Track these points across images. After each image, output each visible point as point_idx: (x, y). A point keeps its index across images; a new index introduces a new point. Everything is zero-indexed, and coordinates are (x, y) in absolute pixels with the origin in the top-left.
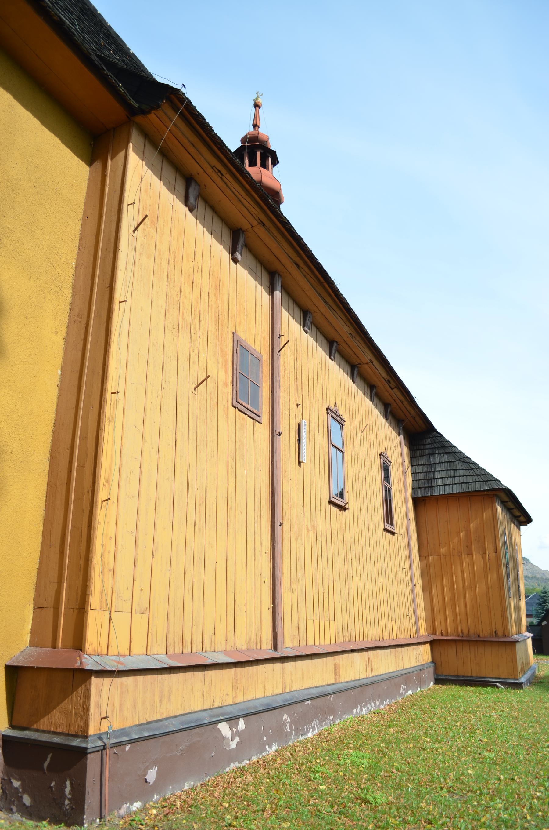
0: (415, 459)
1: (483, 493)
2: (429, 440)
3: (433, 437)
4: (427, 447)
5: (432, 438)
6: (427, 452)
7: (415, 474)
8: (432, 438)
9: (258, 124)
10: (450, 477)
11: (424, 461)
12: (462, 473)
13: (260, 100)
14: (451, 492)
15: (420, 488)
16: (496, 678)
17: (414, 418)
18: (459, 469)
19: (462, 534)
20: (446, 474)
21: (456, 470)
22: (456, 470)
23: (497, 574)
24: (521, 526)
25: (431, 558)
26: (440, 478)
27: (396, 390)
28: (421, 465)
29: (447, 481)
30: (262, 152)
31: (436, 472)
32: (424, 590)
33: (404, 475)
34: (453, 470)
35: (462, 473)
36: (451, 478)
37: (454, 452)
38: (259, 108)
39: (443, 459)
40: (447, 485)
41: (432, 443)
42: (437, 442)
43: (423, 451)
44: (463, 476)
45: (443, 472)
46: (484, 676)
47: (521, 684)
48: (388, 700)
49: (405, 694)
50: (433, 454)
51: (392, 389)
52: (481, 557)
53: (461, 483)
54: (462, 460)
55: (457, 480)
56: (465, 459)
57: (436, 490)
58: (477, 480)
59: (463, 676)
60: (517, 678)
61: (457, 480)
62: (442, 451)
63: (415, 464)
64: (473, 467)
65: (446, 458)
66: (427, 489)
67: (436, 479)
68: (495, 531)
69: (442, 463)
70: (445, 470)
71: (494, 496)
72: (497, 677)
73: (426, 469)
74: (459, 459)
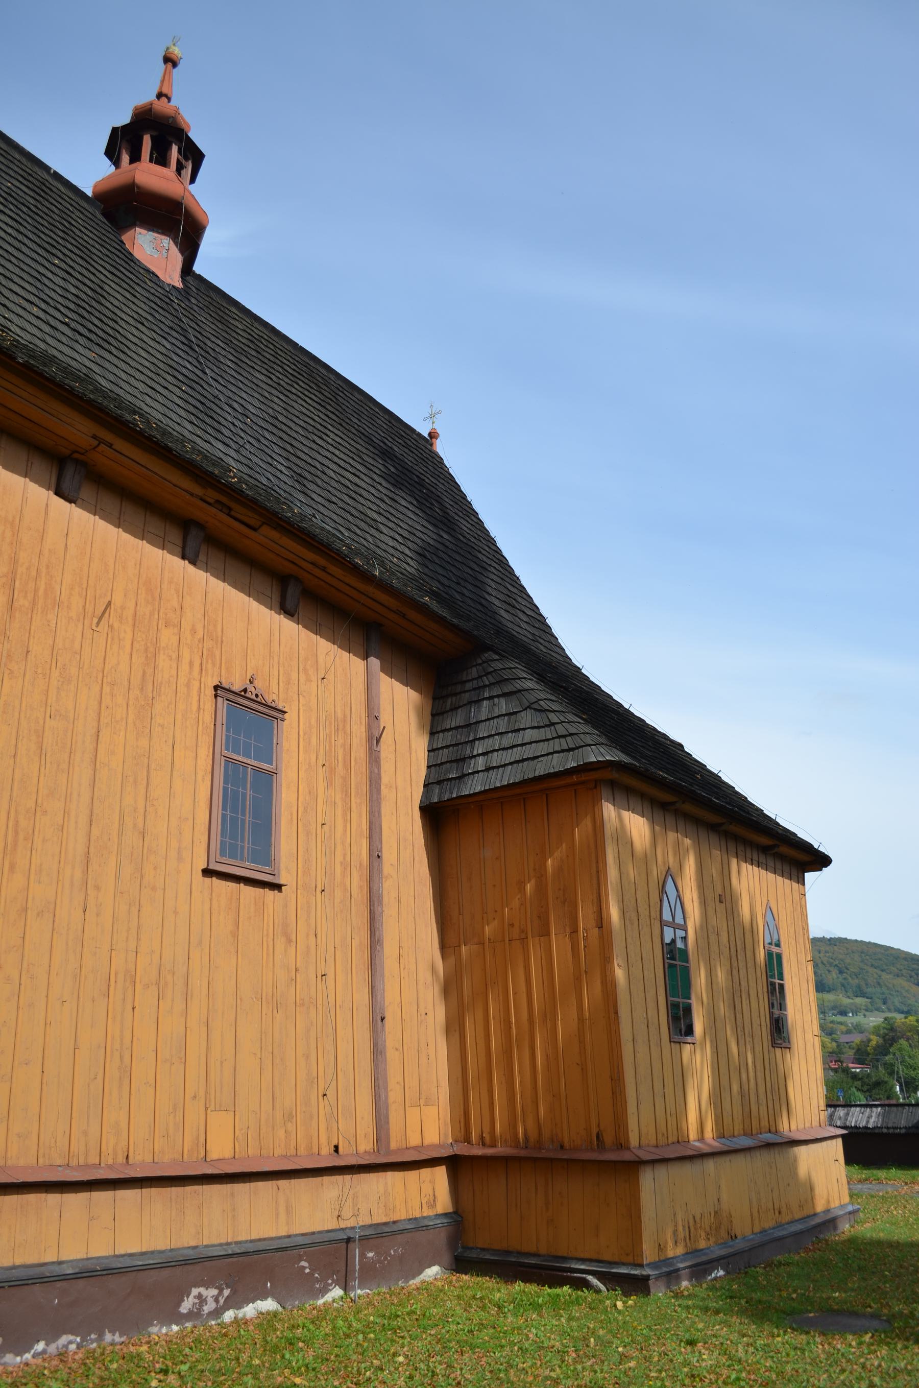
0: (441, 717)
1: (568, 780)
2: (474, 669)
3: (484, 662)
4: (468, 686)
5: (480, 664)
6: (466, 697)
7: (437, 752)
8: (480, 664)
9: (165, 91)
10: (504, 749)
11: (457, 719)
12: (529, 735)
13: (176, 51)
14: (498, 785)
15: (439, 782)
16: (591, 1260)
17: (404, 616)
18: (524, 729)
19: (528, 886)
20: (496, 742)
21: (518, 730)
22: (518, 730)
23: (602, 982)
24: (806, 874)
25: (463, 948)
26: (483, 754)
27: (266, 530)
28: (451, 729)
29: (496, 759)
30: (155, 133)
31: (477, 742)
32: (448, 1030)
33: (371, 748)
34: (512, 732)
35: (529, 735)
36: (505, 752)
37: (520, 691)
38: (175, 65)
39: (496, 710)
40: (493, 768)
41: (480, 677)
42: (490, 673)
43: (458, 697)
44: (531, 743)
45: (491, 739)
46: (565, 1255)
47: (647, 1278)
48: (64, 1339)
49: (217, 1313)
50: (479, 701)
51: (255, 529)
52: (567, 939)
53: (523, 760)
54: (534, 706)
55: (516, 754)
56: (542, 703)
57: (470, 782)
58: (557, 748)
59: (520, 1253)
60: (639, 1262)
61: (516, 754)
62: (496, 691)
63: (439, 729)
64: (555, 720)
65: (503, 706)
66: (453, 782)
67: (474, 757)
68: (598, 872)
69: (493, 718)
70: (497, 734)
71: (597, 783)
72: (595, 1257)
73: (458, 736)
74: (528, 704)
